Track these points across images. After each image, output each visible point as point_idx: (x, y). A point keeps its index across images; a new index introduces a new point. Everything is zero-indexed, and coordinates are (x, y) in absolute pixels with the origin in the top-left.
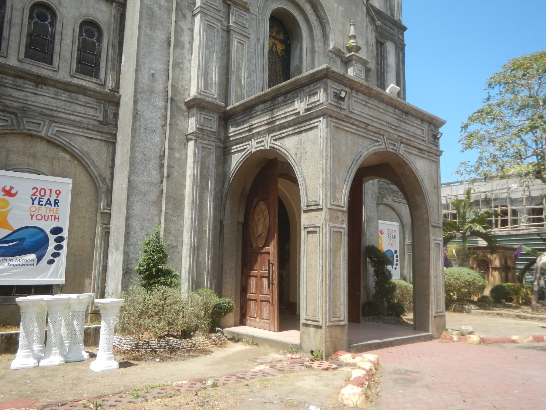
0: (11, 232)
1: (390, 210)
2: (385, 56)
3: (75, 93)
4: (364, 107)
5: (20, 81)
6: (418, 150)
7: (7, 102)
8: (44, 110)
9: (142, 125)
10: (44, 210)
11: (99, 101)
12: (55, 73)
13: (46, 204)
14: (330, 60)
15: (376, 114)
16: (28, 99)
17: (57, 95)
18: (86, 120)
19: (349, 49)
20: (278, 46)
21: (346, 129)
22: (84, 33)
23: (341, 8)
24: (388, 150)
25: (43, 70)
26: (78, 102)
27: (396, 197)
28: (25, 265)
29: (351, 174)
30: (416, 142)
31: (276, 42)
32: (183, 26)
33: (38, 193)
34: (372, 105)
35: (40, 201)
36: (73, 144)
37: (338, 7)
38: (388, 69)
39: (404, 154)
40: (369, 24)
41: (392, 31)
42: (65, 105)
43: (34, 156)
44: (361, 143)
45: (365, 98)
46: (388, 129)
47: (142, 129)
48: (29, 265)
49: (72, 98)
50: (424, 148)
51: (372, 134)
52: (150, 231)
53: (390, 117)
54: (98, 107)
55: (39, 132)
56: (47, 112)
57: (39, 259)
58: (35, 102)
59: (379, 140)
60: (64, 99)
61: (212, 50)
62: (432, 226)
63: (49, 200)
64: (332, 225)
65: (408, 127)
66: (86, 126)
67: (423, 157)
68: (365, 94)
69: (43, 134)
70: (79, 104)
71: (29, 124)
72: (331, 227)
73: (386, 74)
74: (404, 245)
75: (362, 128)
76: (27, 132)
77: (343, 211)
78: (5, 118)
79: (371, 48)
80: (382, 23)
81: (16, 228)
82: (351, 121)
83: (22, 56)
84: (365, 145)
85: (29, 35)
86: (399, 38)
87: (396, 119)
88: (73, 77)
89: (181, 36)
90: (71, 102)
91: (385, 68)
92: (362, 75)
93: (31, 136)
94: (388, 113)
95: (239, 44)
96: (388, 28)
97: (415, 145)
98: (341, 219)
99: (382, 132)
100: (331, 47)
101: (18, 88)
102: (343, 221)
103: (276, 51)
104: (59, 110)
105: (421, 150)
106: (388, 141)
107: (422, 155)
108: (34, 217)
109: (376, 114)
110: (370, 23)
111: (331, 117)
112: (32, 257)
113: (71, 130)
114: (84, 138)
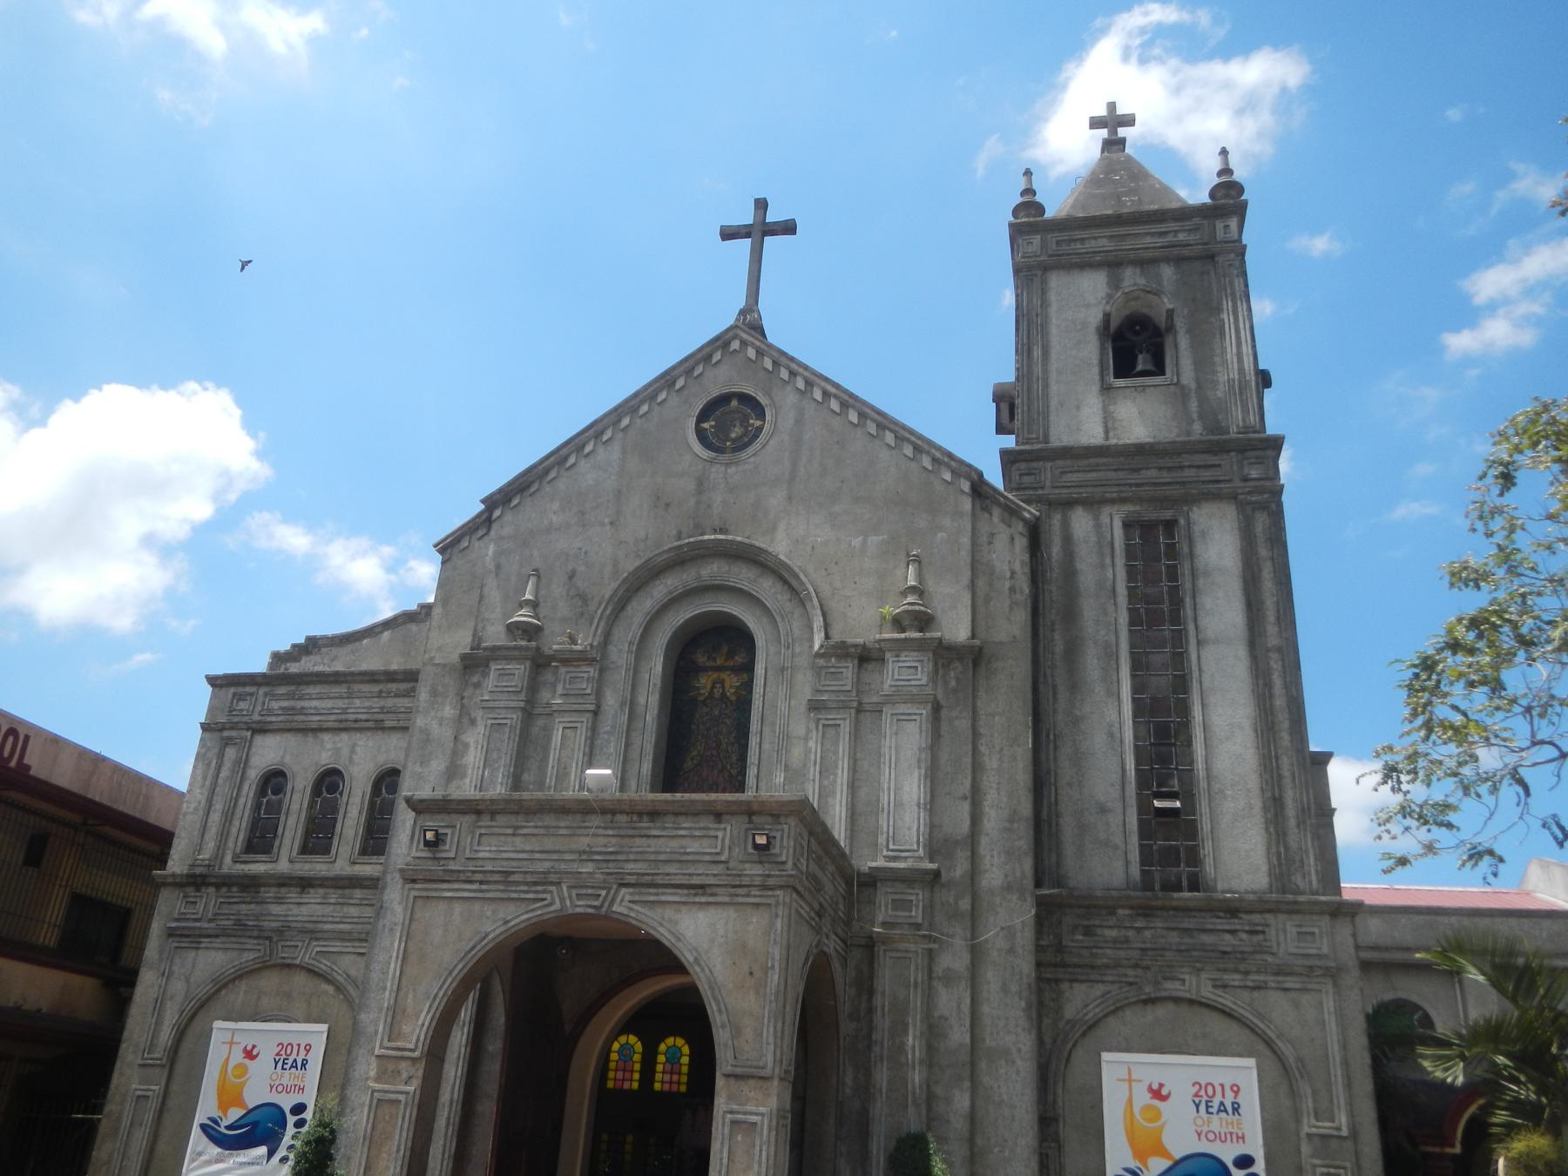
0: (244, 1112)
1: (1215, 1016)
2: (1186, 550)
3: (349, 888)
4: (509, 839)
5: (283, 890)
6: (686, 891)
7: (266, 924)
8: (306, 925)
9: (388, 924)
10: (287, 1078)
12: (331, 865)
13: (292, 1067)
14: (818, 675)
15: (549, 844)
16: (290, 913)
17: (325, 898)
18: (360, 926)
19: (898, 623)
20: (727, 684)
23: (874, 540)
24: (570, 911)
25: (317, 867)
26: (351, 901)
27: (1236, 971)
28: (253, 1164)
29: (446, 979)
30: (676, 874)
31: (724, 675)
32: (468, 740)
33: (283, 1052)
34: (536, 827)
35: (284, 1063)
36: (336, 968)
37: (865, 542)
38: (1201, 582)
39: (631, 909)
40: (1002, 527)
41: (1207, 474)
42: (334, 911)
43: (288, 996)
44: (489, 913)
45: (519, 820)
46: (575, 867)
47: (387, 930)
48: (258, 1164)
49: (344, 898)
50: (712, 881)
51: (525, 888)
53: (596, 837)
55: (292, 958)
56: (310, 926)
57: (271, 1154)
58: (297, 916)
59: (544, 896)
60: (332, 901)
61: (496, 765)
62: (727, 1076)
63: (295, 1060)
64: (377, 1086)
65: (654, 844)
66: (356, 936)
67: (709, 904)
68: (517, 813)
69: (297, 962)
70: (353, 905)
71: (286, 949)
72: (373, 1091)
73: (1188, 600)
74: (1299, 1139)
75: (496, 882)
76: (279, 961)
77: (413, 1060)
78: (258, 947)
79: (1008, 584)
80: (1160, 469)
81: (251, 1107)
82: (462, 877)
83: (294, 853)
84: (502, 915)
85: (311, 820)
86: (1246, 479)
87: (613, 836)
88: (354, 863)
89: (463, 756)
90: (343, 904)
91: (1188, 585)
92: (919, 676)
93: (289, 966)
94: (586, 832)
95: (568, 731)
96: (1193, 472)
97: (673, 882)
98: (405, 1075)
99: (553, 878)
100: (817, 647)
101: (279, 901)
102: (410, 1078)
103: (724, 694)
104: (325, 919)
105: (702, 887)
106: (574, 892)
107: (703, 899)
108: (274, 1089)
109: (549, 844)
110: (1003, 521)
111: (414, 881)
112: (262, 1150)
113: (336, 946)
114: (353, 957)
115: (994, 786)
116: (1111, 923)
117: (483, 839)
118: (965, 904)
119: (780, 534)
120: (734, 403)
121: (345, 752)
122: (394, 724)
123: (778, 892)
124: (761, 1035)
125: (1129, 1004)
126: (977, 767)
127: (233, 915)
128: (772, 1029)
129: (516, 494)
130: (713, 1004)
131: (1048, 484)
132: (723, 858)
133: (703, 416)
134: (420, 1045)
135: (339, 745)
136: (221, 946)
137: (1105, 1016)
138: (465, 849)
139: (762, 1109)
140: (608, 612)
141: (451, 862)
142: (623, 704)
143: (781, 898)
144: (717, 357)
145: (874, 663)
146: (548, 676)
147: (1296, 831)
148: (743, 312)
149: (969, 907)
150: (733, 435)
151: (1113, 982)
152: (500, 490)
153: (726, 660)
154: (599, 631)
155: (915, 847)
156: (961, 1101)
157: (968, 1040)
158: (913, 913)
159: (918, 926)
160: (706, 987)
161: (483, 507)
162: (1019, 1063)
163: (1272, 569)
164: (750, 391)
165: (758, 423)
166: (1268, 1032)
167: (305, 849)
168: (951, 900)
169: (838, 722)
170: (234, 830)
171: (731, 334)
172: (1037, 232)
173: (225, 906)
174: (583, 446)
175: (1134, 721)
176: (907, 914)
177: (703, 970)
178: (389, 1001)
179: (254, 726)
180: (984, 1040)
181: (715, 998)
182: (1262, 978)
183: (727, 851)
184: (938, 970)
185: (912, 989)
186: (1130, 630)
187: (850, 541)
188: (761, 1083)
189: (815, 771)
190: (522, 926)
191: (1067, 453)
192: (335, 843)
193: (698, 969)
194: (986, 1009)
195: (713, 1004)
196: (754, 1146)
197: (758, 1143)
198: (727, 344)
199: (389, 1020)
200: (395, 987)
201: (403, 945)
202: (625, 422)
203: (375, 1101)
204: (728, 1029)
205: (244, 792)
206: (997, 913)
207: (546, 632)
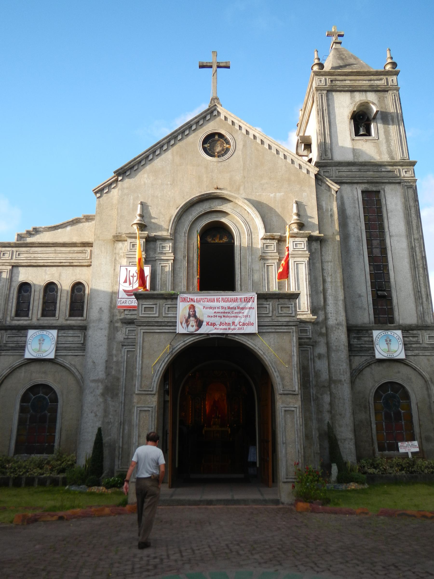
11: (82, 331)
21: (158, 331)
22: (75, 291)
37: (275, 195)
38: (389, 214)
43: (45, 373)
52: (97, 413)
54: (80, 335)
88: (67, 320)
95: (163, 267)
114: (72, 356)
115: (330, 288)
116: (367, 336)
117: (170, 309)
118: (324, 330)
119: (242, 191)
120: (217, 137)
121: (57, 275)
122: (78, 264)
123: (293, 328)
124: (292, 379)
125: (373, 363)
126: (324, 281)
127: (15, 341)
128: (296, 377)
129: (128, 170)
130: (273, 369)
131: (334, 176)
132: (270, 315)
133: (205, 142)
134: (155, 389)
135: (54, 272)
136: (11, 354)
137: (366, 367)
138: (162, 313)
139: (296, 406)
140: (175, 220)
141: (157, 318)
142: (184, 257)
143: (294, 330)
144: (208, 117)
145: (283, 242)
146: (152, 245)
147: (426, 302)
148: (213, 99)
149: (325, 331)
150: (218, 150)
151: (368, 356)
152: (121, 168)
153: (219, 240)
154: (173, 228)
155: (307, 310)
156: (327, 398)
157: (328, 378)
158: (308, 334)
159: (310, 338)
160: (269, 363)
161: (114, 175)
162: (345, 385)
163: (414, 210)
164: (223, 132)
165: (228, 146)
166: (420, 369)
167: (43, 315)
168: (319, 329)
169: (272, 264)
170: (10, 308)
171: (214, 108)
172: (322, 75)
173: (11, 338)
174: (155, 151)
175: (369, 265)
176: (306, 334)
177: (267, 357)
178: (138, 373)
179: (13, 264)
180: (332, 377)
181: (273, 367)
182: (417, 352)
183: (271, 313)
184: (316, 354)
185: (310, 361)
186: (366, 231)
187: (270, 195)
188: (294, 396)
189: (265, 282)
190: (191, 343)
191: (340, 164)
192: (57, 312)
193: (265, 356)
194: (332, 367)
195: (273, 369)
196: (294, 418)
197: (295, 417)
198: (212, 112)
199: (139, 380)
200: (140, 367)
201: (141, 351)
202: (172, 142)
203: (139, 411)
204: (279, 378)
205: (12, 292)
206: (334, 333)
207: (147, 228)
